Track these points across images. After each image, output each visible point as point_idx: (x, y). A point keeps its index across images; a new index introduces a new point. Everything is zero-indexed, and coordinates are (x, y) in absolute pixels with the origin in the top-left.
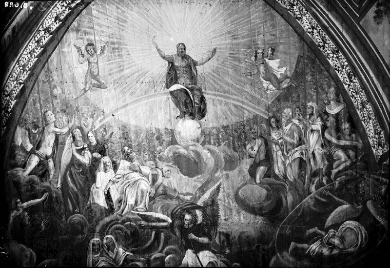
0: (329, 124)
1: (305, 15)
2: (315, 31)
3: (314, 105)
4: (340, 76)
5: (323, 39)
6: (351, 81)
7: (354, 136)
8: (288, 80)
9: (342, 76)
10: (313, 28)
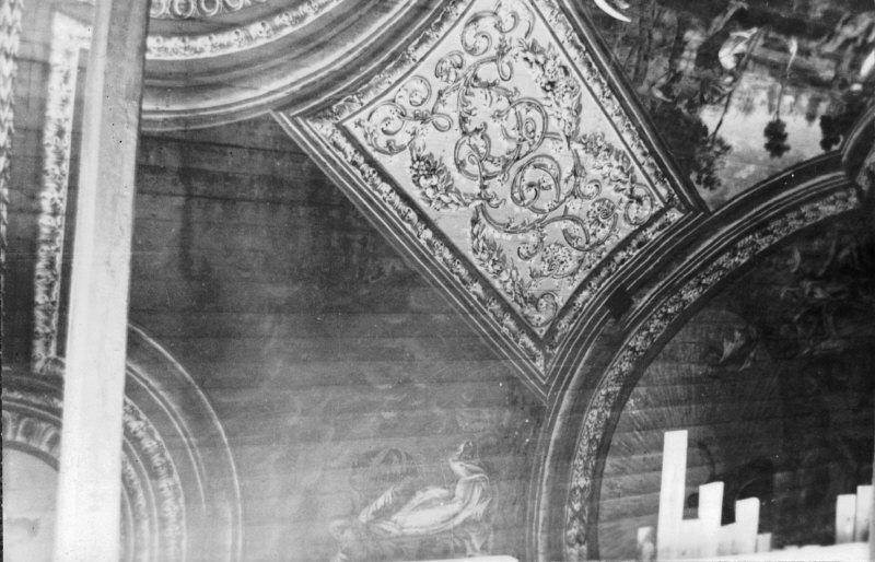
0: (809, 270)
1: (681, 296)
2: (704, 281)
3: (785, 289)
4: (763, 248)
5: (715, 270)
6: (771, 232)
7: (828, 234)
8: (750, 327)
9: (764, 244)
10: (700, 284)
